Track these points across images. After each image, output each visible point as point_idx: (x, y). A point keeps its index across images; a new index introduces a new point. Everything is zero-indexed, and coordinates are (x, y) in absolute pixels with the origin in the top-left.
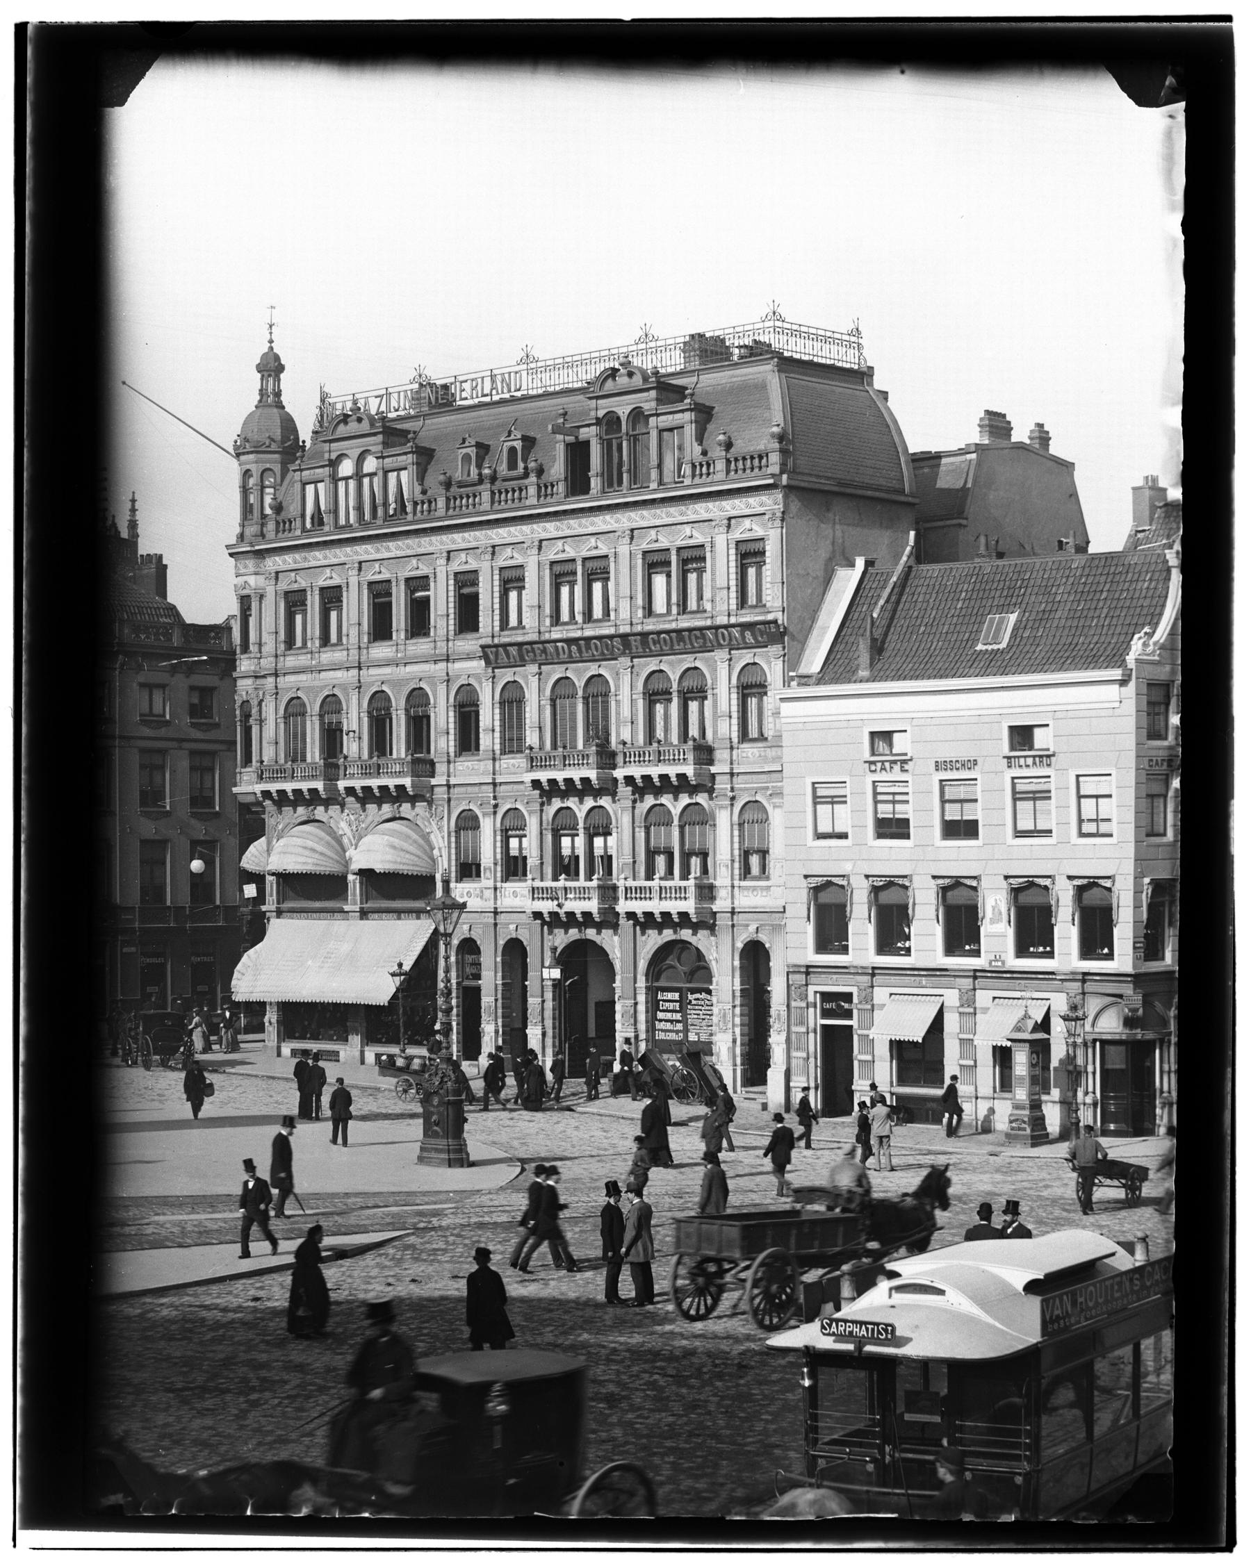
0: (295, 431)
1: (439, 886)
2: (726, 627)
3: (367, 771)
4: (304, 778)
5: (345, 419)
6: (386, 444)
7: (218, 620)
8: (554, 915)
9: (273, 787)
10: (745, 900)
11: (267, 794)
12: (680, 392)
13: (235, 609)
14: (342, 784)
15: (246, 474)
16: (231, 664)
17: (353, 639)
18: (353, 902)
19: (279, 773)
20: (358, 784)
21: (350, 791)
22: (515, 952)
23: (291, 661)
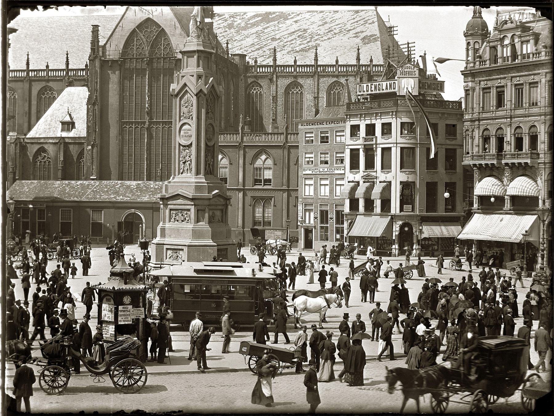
0: (486, 27)
1: (540, 202)
3: (513, 156)
4: (489, 159)
5: (506, 22)
6: (523, 31)
7: (457, 99)
9: (477, 162)
11: (475, 165)
12: (529, 29)
13: (463, 94)
14: (503, 162)
15: (468, 44)
16: (462, 115)
17: (509, 107)
18: (508, 205)
19: (480, 157)
20: (510, 161)
21: (507, 164)
23: (484, 115)
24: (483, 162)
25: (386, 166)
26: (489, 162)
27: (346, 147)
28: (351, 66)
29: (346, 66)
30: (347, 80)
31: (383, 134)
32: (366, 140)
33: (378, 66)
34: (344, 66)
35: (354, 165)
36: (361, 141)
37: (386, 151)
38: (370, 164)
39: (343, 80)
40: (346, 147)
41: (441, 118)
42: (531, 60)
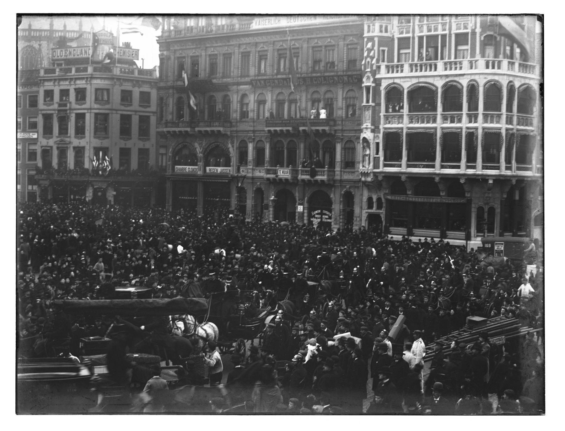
2: (342, 76)
8: (274, 179)
10: (346, 177)
13: (158, 63)
21: (200, 132)
22: (259, 193)
24: (177, 130)
25: (80, 131)
26: (183, 129)
27: (40, 112)
28: (45, 31)
29: (40, 31)
30: (40, 45)
31: (77, 99)
32: (60, 105)
33: (72, 31)
34: (37, 30)
35: (48, 131)
36: (56, 106)
37: (80, 117)
38: (63, 130)
39: (36, 46)
40: (40, 112)
41: (134, 86)
42: (225, 31)
